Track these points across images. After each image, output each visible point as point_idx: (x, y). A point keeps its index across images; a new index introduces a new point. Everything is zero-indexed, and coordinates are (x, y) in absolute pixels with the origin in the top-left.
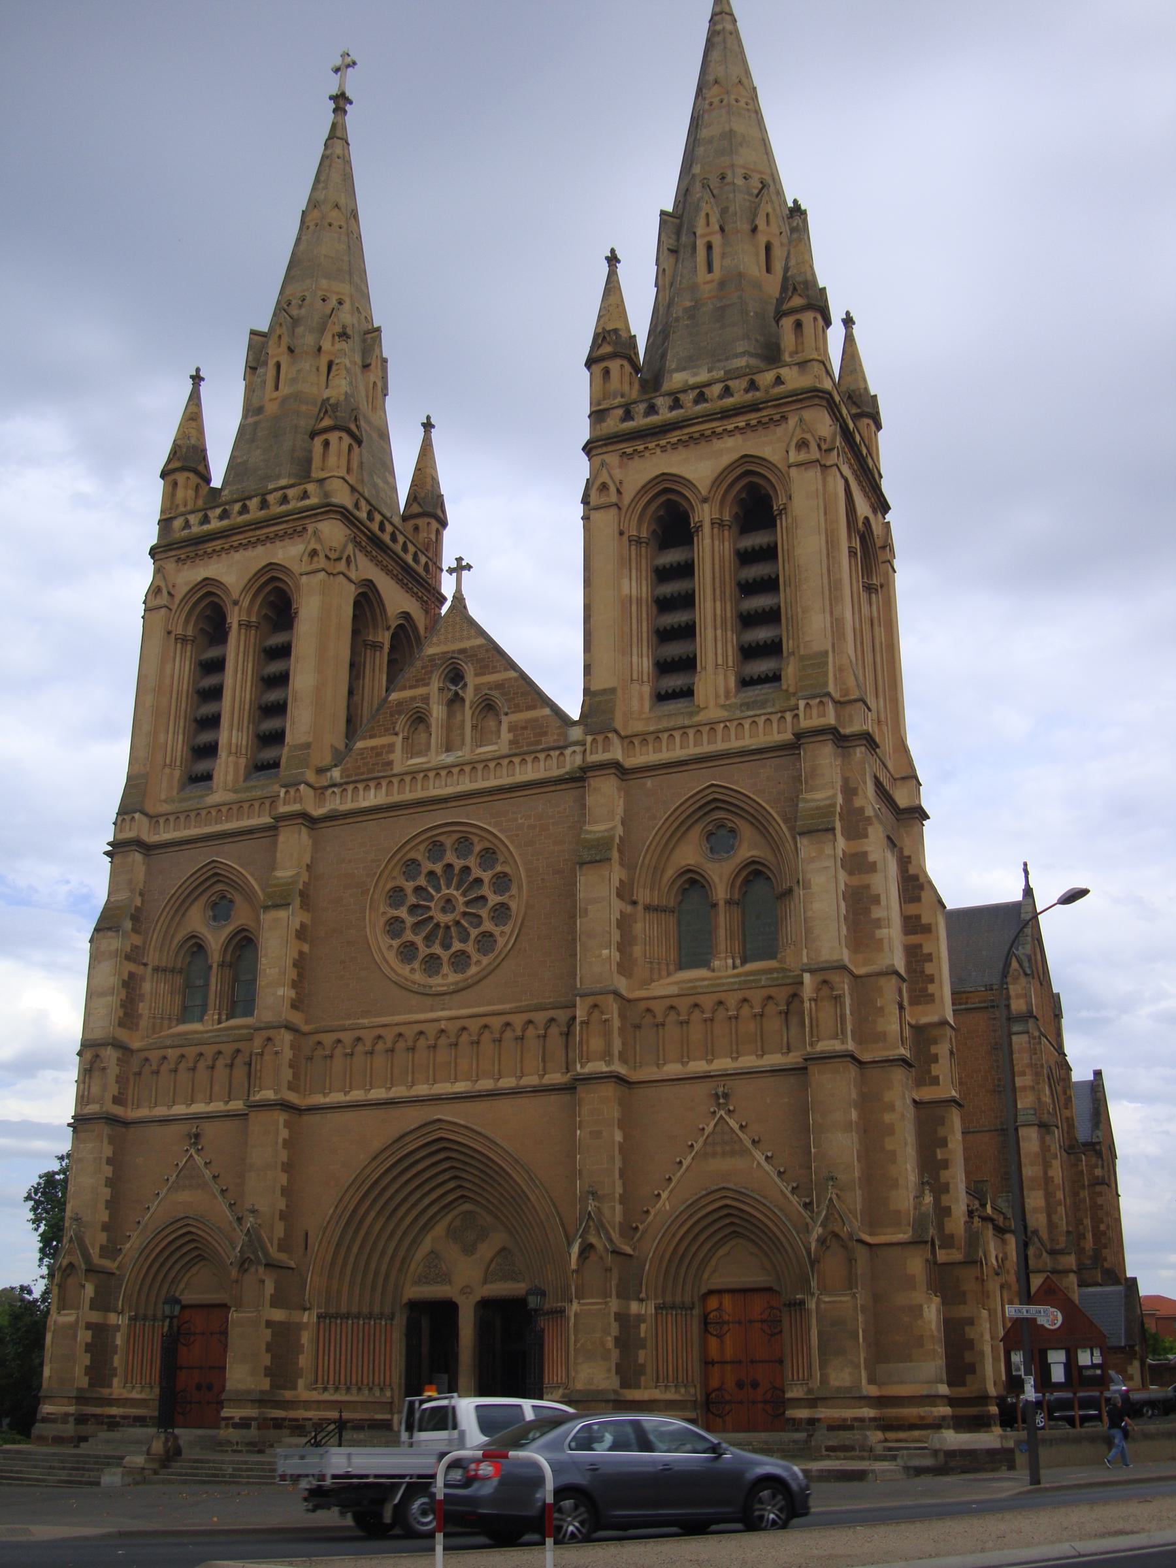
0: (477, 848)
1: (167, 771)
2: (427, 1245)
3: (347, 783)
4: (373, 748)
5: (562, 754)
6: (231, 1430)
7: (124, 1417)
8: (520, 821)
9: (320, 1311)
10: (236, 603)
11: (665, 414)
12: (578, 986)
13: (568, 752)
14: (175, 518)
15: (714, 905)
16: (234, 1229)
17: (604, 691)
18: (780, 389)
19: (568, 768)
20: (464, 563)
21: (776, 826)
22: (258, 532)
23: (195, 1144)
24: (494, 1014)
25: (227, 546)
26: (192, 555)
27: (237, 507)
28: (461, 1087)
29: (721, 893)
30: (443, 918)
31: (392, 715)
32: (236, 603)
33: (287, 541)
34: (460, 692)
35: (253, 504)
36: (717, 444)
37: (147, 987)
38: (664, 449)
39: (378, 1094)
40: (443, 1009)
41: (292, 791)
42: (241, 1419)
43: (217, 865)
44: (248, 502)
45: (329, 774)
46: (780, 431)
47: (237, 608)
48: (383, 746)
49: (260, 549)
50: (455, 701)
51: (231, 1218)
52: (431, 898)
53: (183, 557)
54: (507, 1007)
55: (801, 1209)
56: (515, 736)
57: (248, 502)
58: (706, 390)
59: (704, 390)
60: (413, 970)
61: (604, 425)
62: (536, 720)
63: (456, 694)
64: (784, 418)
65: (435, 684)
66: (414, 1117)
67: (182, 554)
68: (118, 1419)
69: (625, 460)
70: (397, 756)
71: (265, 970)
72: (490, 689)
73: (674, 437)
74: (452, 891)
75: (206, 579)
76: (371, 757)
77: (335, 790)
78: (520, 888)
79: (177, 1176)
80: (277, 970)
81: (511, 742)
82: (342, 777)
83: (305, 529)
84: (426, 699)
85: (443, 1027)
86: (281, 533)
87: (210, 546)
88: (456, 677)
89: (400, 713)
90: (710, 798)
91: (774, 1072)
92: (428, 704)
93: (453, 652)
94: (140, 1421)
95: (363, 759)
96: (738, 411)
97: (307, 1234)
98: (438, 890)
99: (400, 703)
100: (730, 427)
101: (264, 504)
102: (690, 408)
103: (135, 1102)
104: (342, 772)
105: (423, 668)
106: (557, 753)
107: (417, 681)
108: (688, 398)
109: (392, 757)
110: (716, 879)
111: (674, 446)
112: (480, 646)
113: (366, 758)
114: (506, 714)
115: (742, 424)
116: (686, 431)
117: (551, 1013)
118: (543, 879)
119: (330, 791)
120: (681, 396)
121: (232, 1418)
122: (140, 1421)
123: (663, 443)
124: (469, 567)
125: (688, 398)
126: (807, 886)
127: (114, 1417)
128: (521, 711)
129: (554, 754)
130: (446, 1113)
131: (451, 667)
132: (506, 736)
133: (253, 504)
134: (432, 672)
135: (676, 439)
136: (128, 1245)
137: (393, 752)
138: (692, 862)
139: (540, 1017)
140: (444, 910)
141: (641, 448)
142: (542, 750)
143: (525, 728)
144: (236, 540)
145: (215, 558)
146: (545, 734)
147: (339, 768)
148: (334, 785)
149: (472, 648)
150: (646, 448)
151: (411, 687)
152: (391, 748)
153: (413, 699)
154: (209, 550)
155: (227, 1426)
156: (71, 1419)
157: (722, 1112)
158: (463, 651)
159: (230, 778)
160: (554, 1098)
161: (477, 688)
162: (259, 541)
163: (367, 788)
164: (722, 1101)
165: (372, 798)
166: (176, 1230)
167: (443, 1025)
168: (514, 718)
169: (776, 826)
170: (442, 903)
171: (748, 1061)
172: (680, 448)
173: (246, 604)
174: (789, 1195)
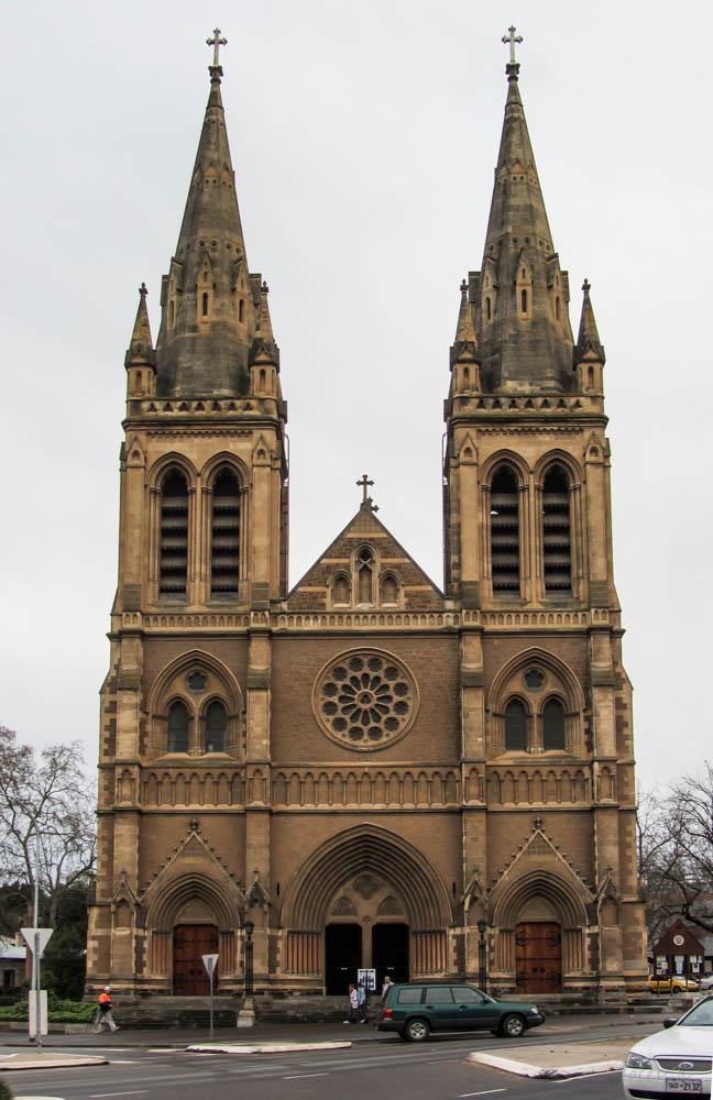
1: (151, 583)
4: (310, 593)
7: (154, 990)
13: (445, 615)
17: (471, 583)
18: (578, 410)
19: (444, 625)
23: (196, 829)
27: (195, 404)
28: (378, 806)
29: (535, 710)
30: (365, 707)
32: (199, 475)
33: (236, 438)
36: (540, 438)
37: (149, 727)
46: (578, 437)
47: (199, 479)
49: (214, 440)
50: (365, 571)
52: (354, 693)
54: (409, 763)
58: (533, 400)
60: (344, 736)
61: (466, 408)
62: (421, 592)
63: (365, 566)
64: (581, 430)
65: (354, 558)
66: (350, 822)
70: (328, 600)
83: (251, 433)
84: (347, 566)
87: (175, 429)
88: (365, 554)
104: (289, 605)
109: (325, 600)
111: (512, 433)
112: (384, 538)
129: (436, 615)
137: (325, 597)
141: (490, 429)
142: (428, 612)
146: (429, 602)
148: (284, 613)
149: (378, 538)
151: (336, 557)
152: (324, 595)
153: (338, 565)
156: (132, 992)
159: (203, 596)
161: (383, 565)
165: (311, 625)
168: (408, 588)
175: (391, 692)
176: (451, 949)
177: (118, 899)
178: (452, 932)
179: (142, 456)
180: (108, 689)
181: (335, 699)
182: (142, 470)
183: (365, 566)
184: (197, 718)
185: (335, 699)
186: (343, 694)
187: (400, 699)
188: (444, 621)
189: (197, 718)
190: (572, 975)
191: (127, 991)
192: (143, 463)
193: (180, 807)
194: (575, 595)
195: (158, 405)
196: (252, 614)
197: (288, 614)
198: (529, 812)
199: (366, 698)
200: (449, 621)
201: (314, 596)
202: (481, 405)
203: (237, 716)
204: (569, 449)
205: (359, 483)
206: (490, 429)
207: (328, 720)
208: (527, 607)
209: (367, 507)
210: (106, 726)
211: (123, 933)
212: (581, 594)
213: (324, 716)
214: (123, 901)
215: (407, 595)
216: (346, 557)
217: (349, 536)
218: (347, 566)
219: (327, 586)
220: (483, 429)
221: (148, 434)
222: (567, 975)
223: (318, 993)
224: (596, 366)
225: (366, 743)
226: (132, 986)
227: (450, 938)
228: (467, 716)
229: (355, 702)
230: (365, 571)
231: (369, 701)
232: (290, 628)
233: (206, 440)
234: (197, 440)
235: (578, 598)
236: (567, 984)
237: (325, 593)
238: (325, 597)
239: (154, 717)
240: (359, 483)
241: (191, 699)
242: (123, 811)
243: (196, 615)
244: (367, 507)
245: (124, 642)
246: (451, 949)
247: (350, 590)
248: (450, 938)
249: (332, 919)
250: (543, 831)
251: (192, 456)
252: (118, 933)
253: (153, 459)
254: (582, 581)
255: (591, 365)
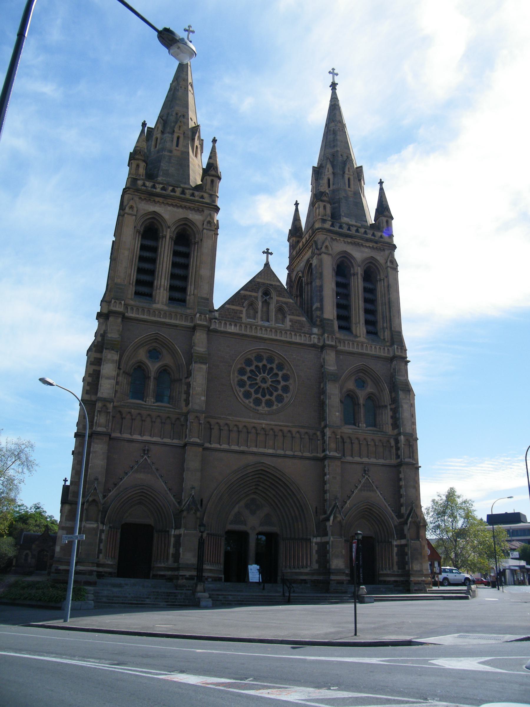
0: (276, 362)
2: (236, 509)
3: (222, 320)
4: (233, 310)
5: (310, 337)
6: (185, 580)
7: (106, 572)
8: (295, 356)
9: (207, 532)
10: (169, 227)
11: (336, 229)
12: (328, 423)
13: (313, 336)
14: (139, 180)
15: (359, 404)
16: (167, 494)
17: (329, 320)
18: (381, 239)
19: (312, 342)
20: (266, 251)
21: (382, 384)
22: (180, 203)
23: (147, 454)
24: (285, 426)
25: (165, 202)
26: (148, 199)
27: (170, 188)
28: (271, 451)
29: (361, 401)
30: (264, 385)
31: (241, 299)
32: (169, 227)
33: (193, 212)
34: (267, 300)
35: (178, 190)
36: (363, 249)
38: (345, 242)
39: (236, 448)
40: (263, 420)
41: (203, 316)
42: (189, 576)
43: (159, 335)
44: (176, 189)
45: (213, 314)
46: (382, 253)
47: (169, 230)
48: (237, 310)
49: (180, 210)
50: (266, 303)
51: (166, 489)
52: (257, 376)
53: (143, 198)
54: (290, 424)
55: (391, 512)
56: (292, 324)
57: (176, 189)
58: (359, 229)
59: (351, 227)
60: (250, 402)
61: (324, 225)
62: (300, 321)
63: (266, 300)
64: (384, 250)
65: (260, 294)
66: (251, 459)
67: (143, 196)
68: (103, 573)
69: (332, 240)
70: (244, 316)
71: (195, 387)
72: (283, 303)
73: (349, 240)
74: (262, 375)
75: (154, 212)
76: (232, 313)
77: (216, 321)
78: (295, 381)
79: (138, 467)
80: (201, 389)
81: (290, 326)
82: (219, 317)
83: (203, 211)
84: (256, 298)
85: (263, 427)
86: (192, 208)
87: (157, 199)
88: (266, 293)
89: (245, 300)
90: (361, 368)
91: (383, 465)
92: (257, 300)
93: (267, 284)
94: (111, 574)
95: (229, 312)
96: (370, 241)
97: (202, 501)
98: (260, 374)
99: (245, 296)
100: (368, 245)
101: (173, 191)
102: (345, 231)
103: (113, 429)
104: (219, 314)
105: (255, 285)
106: (308, 336)
107: (252, 289)
108: (354, 229)
109: (241, 315)
110: (360, 396)
111: (348, 243)
112: (278, 285)
113: (230, 312)
114: (289, 315)
115: (371, 246)
116: (353, 240)
117: (306, 430)
118: (303, 380)
119: (214, 320)
120: (351, 228)
121: (185, 575)
122: (111, 574)
123: (345, 240)
124: (271, 254)
125: (354, 229)
126: (402, 407)
127: (101, 572)
128: (295, 316)
129: (307, 336)
130: (267, 461)
131: (266, 289)
132: (288, 324)
133: (178, 190)
134: (259, 289)
135: (350, 241)
136: (110, 494)
138: (352, 388)
139: (303, 431)
140: (266, 382)
141: (338, 238)
142: (303, 333)
143: (296, 323)
144: (170, 201)
145: (158, 204)
146: (304, 327)
147: (218, 313)
148: (216, 319)
149: (275, 285)
150: (340, 239)
151: (249, 291)
152: (241, 312)
153: (251, 296)
154: (157, 200)
155: (182, 579)
156: (95, 573)
157: (367, 476)
158: (271, 285)
159: (165, 300)
160: (307, 461)
161: (278, 302)
162: (181, 207)
163: (231, 325)
164: (367, 472)
165: (232, 329)
166: (136, 490)
167: (264, 426)
168: (292, 317)
169: (382, 384)
170: (261, 379)
171: (373, 460)
172: (350, 244)
173: (173, 229)
174: (388, 507)
175: (280, 378)
176: (314, 552)
177: (91, 499)
178: (315, 540)
179: (135, 209)
180: (94, 349)
181: (245, 378)
182: (134, 217)
183: (266, 300)
184: (152, 378)
185: (245, 378)
186: (250, 375)
187: (285, 383)
188: (312, 339)
189: (152, 378)
190: (385, 572)
191: (91, 573)
192: (135, 213)
193: (137, 437)
194: (382, 338)
195: (147, 184)
196: (198, 315)
197: (219, 320)
198: (362, 463)
199: (264, 380)
200: (315, 340)
201: (235, 312)
202: (332, 225)
203: (181, 380)
204: (378, 258)
205: (264, 252)
206: (338, 238)
207: (240, 391)
208: (358, 339)
209: (267, 265)
210: (90, 374)
211: (92, 526)
212: (386, 337)
213: (238, 388)
214: (94, 500)
215: (291, 321)
216: (255, 292)
217: (258, 280)
218: (256, 298)
219: (244, 307)
220: (334, 238)
221: (140, 198)
222: (381, 572)
223: (220, 579)
224: (389, 220)
225: (263, 409)
226: (95, 568)
227: (314, 544)
228: (330, 398)
229: (258, 382)
230: (266, 303)
231: (266, 382)
232: (219, 329)
233: (175, 209)
234: (169, 208)
235: (384, 339)
236: (382, 579)
237: (242, 311)
238: (242, 314)
239: (124, 372)
240: (264, 252)
241: (149, 364)
242: (99, 434)
243: (160, 311)
244: (267, 265)
245: (111, 319)
246: (314, 552)
247: (257, 312)
248: (314, 544)
249: (230, 527)
250: (369, 476)
251: (166, 216)
252: (88, 526)
253: (142, 212)
254: (386, 330)
255: (388, 219)
